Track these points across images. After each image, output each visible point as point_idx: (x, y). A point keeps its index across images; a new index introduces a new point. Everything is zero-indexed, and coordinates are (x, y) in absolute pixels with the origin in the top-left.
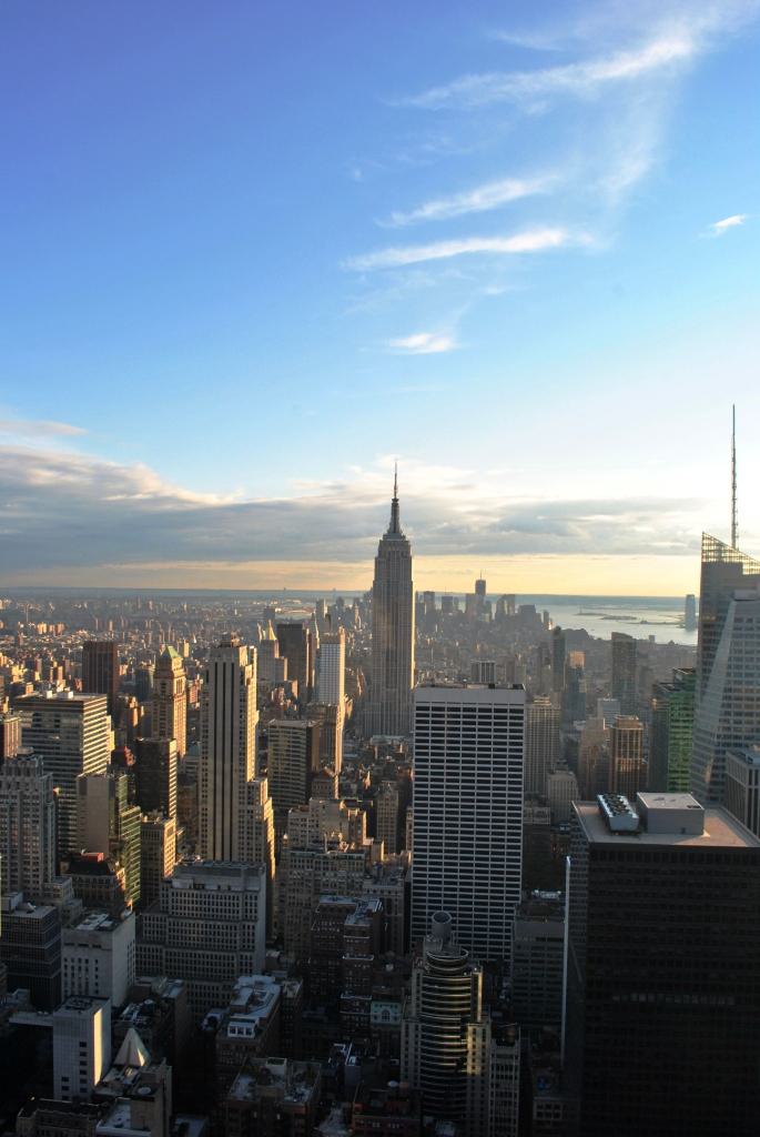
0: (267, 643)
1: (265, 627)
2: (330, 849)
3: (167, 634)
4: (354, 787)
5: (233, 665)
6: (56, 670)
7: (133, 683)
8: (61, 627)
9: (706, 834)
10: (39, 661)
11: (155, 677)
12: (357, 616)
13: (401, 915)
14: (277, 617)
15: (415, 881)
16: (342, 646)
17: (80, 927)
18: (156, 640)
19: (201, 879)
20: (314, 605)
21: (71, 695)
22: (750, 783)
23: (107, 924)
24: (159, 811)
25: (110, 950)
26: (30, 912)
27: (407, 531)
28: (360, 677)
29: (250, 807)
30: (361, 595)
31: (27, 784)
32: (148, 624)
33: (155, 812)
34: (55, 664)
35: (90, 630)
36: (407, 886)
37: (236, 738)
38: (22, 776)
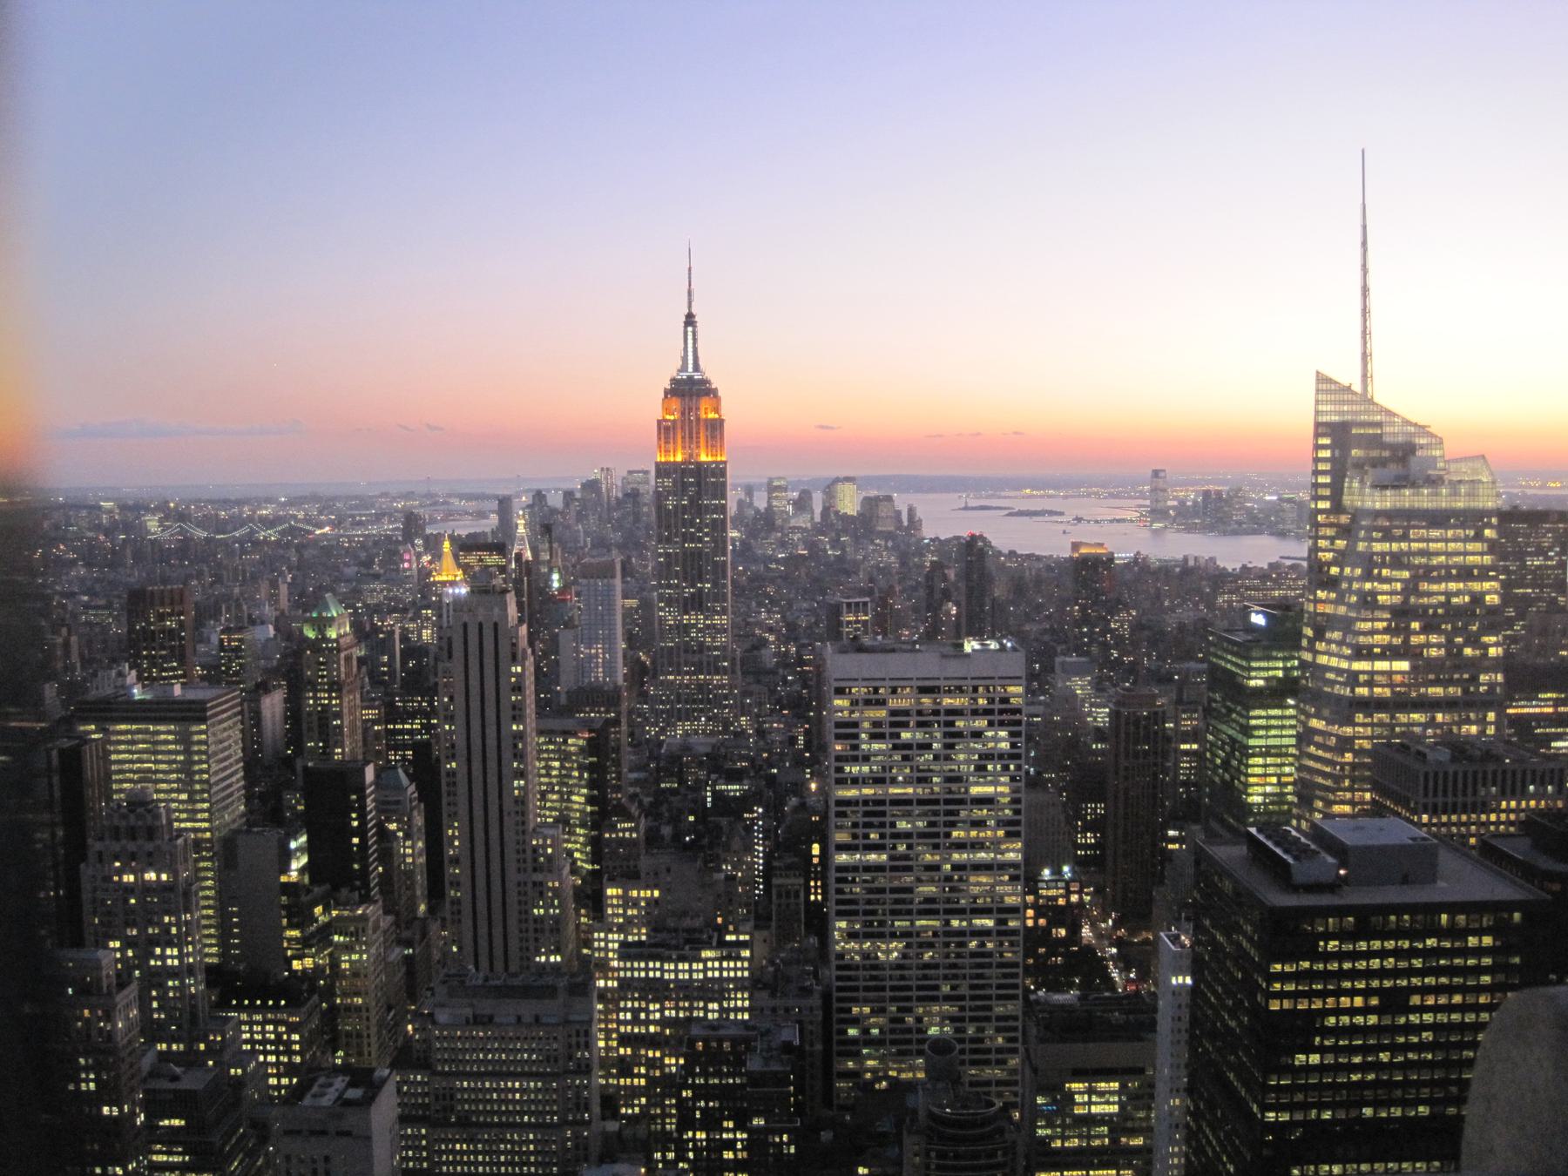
2: (687, 941)
4: (667, 831)
5: (496, 624)
9: (1441, 884)
13: (819, 1047)
15: (840, 989)
17: (307, 1101)
19: (486, 1006)
22: (1426, 795)
23: (354, 1094)
24: (352, 891)
25: (369, 1138)
26: (175, 1078)
29: (538, 877)
31: (150, 854)
33: (344, 892)
36: (827, 997)
37: (507, 754)
38: (140, 842)
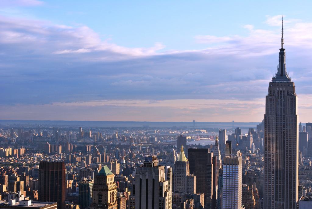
0: (181, 164)
1: (179, 151)
3: (103, 156)
6: (19, 184)
7: (76, 194)
8: (22, 151)
10: (6, 177)
11: (93, 190)
12: (251, 142)
14: (188, 143)
16: (240, 167)
18: (94, 161)
20: (217, 134)
21: (30, 203)
27: (290, 74)
28: (254, 192)
30: (256, 126)
32: (89, 148)
34: (18, 179)
35: (45, 153)
